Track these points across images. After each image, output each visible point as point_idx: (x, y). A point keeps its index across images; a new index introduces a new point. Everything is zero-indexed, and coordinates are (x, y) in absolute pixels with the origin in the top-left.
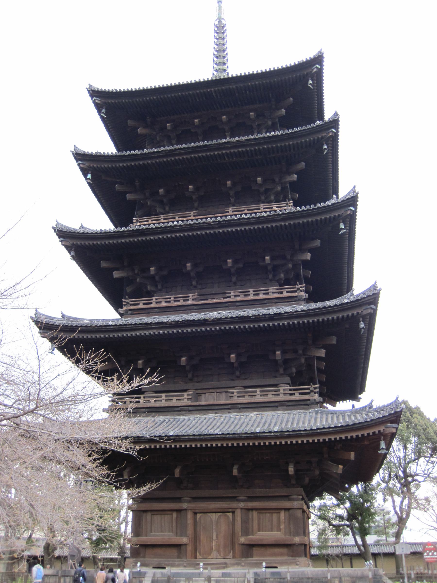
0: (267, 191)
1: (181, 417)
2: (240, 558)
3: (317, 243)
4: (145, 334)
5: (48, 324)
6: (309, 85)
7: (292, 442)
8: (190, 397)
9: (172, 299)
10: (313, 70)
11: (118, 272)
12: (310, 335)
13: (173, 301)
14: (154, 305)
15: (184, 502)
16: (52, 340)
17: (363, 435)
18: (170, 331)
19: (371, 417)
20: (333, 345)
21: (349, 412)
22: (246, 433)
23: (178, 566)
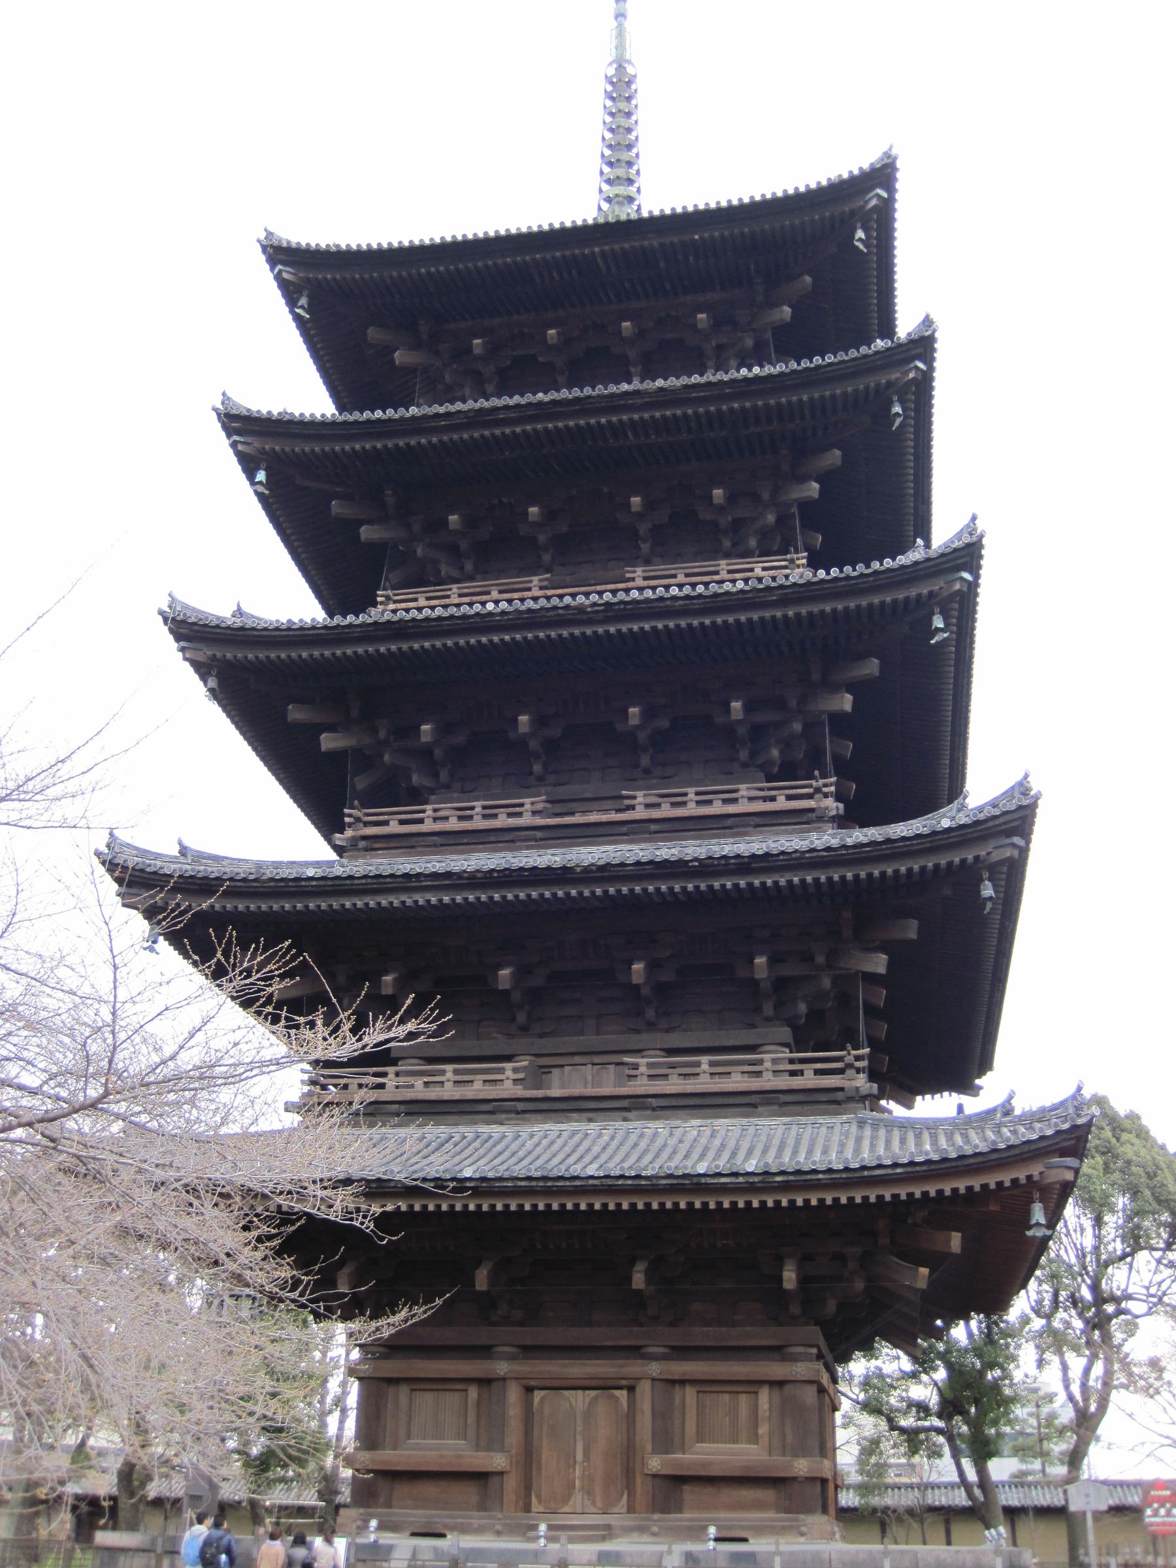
0: (738, 525)
1: (496, 1130)
2: (647, 1512)
3: (872, 667)
4: (403, 903)
5: (142, 871)
6: (857, 244)
7: (792, 1202)
8: (521, 1075)
9: (478, 810)
10: (867, 202)
11: (332, 735)
12: (847, 914)
13: (480, 817)
14: (428, 826)
15: (500, 1359)
16: (150, 913)
17: (985, 1187)
18: (471, 898)
19: (1008, 1139)
20: (909, 942)
21: (950, 1125)
22: (670, 1176)
23: (480, 1530)
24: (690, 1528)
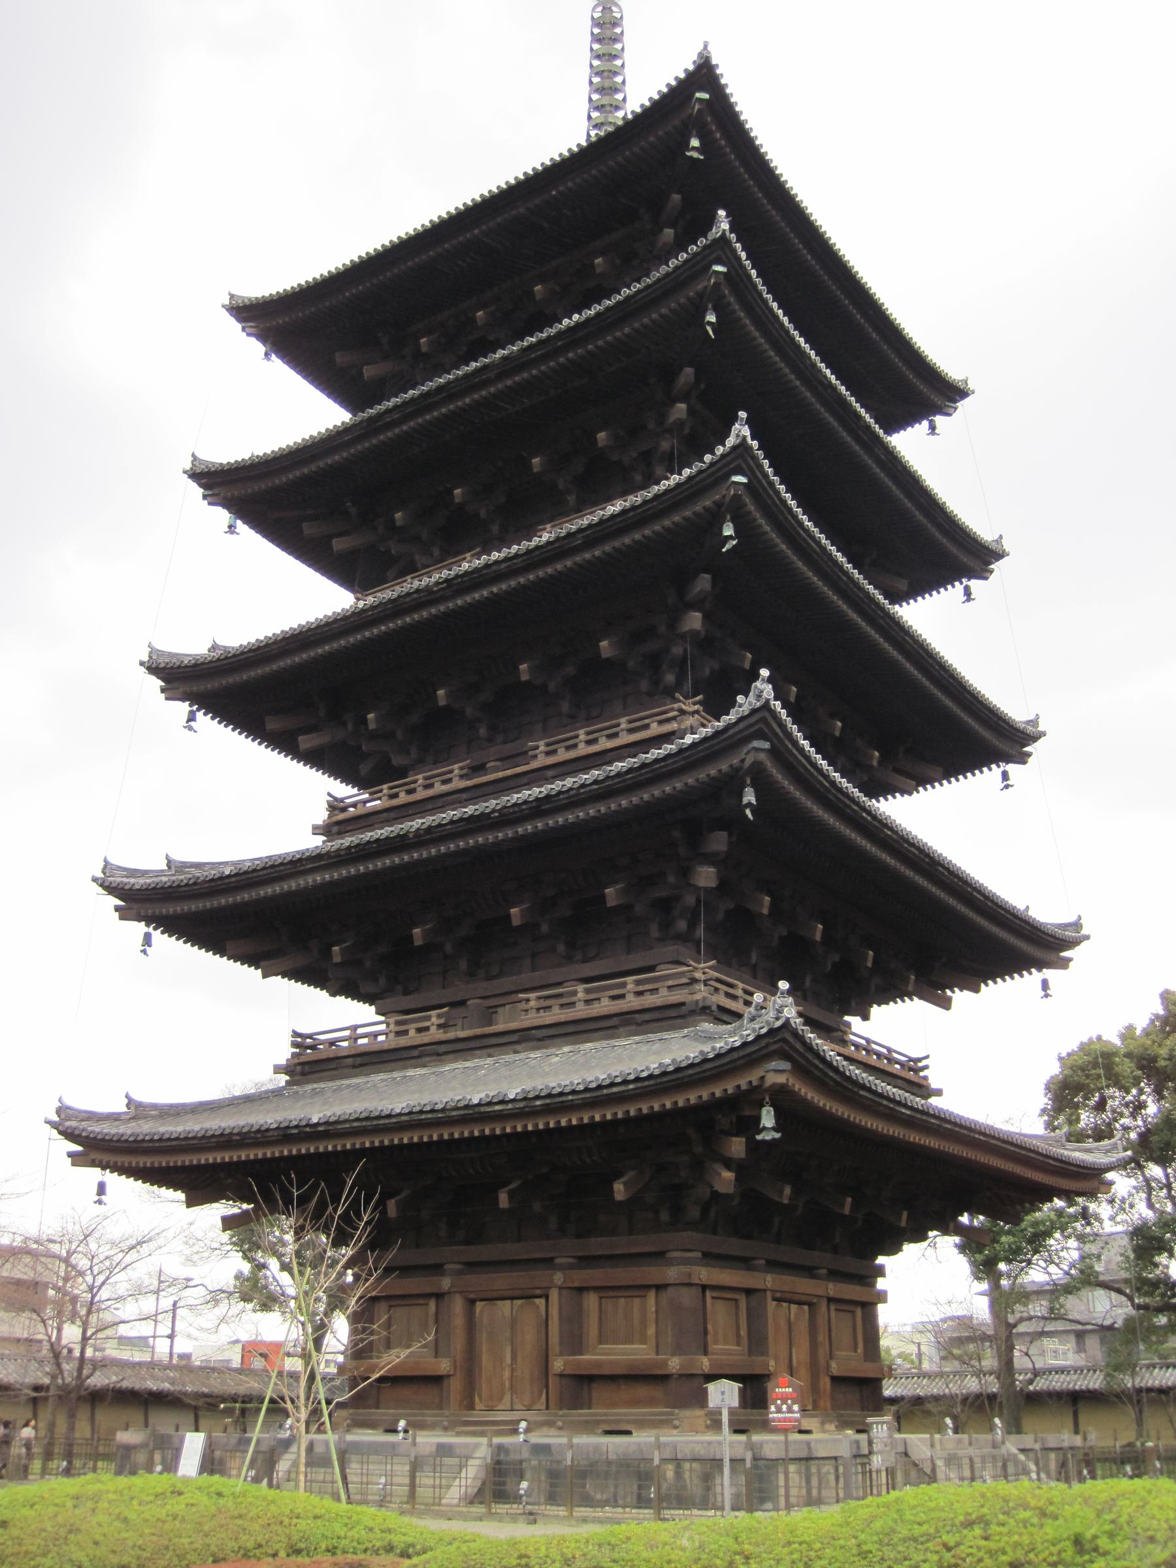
3: (703, 583)
12: (677, 834)
24: (586, 1422)
